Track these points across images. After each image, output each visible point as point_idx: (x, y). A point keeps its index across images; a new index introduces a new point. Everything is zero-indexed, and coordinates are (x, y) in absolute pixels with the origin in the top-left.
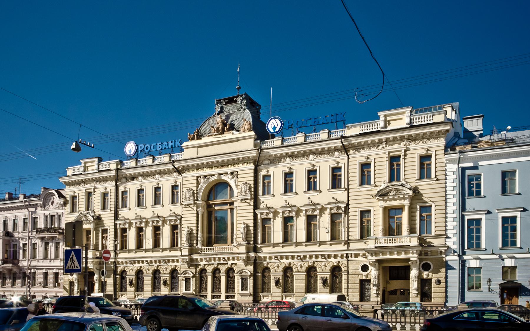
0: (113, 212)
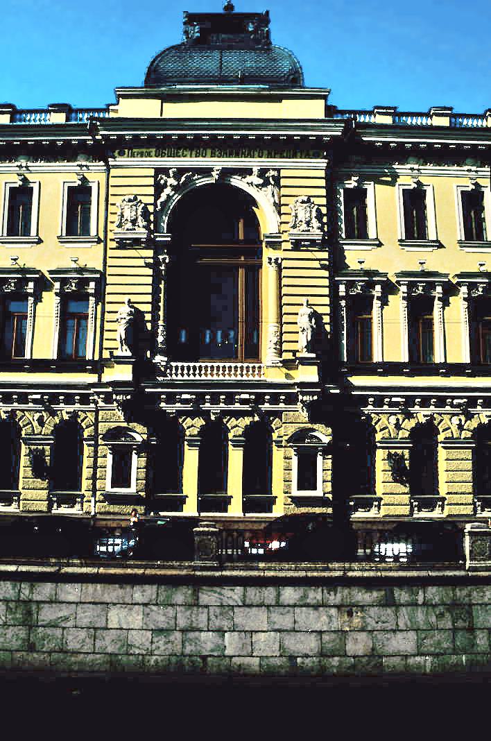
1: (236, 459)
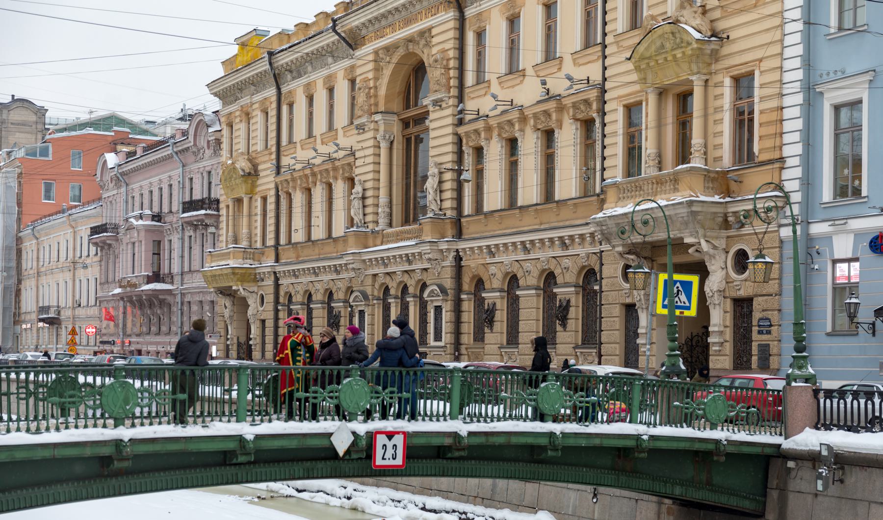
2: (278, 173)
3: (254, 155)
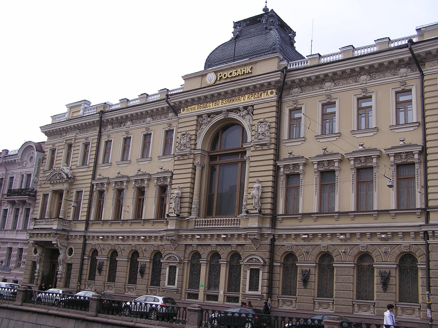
0: (92, 169)
1: (224, 272)
2: (94, 178)
3: (73, 167)
